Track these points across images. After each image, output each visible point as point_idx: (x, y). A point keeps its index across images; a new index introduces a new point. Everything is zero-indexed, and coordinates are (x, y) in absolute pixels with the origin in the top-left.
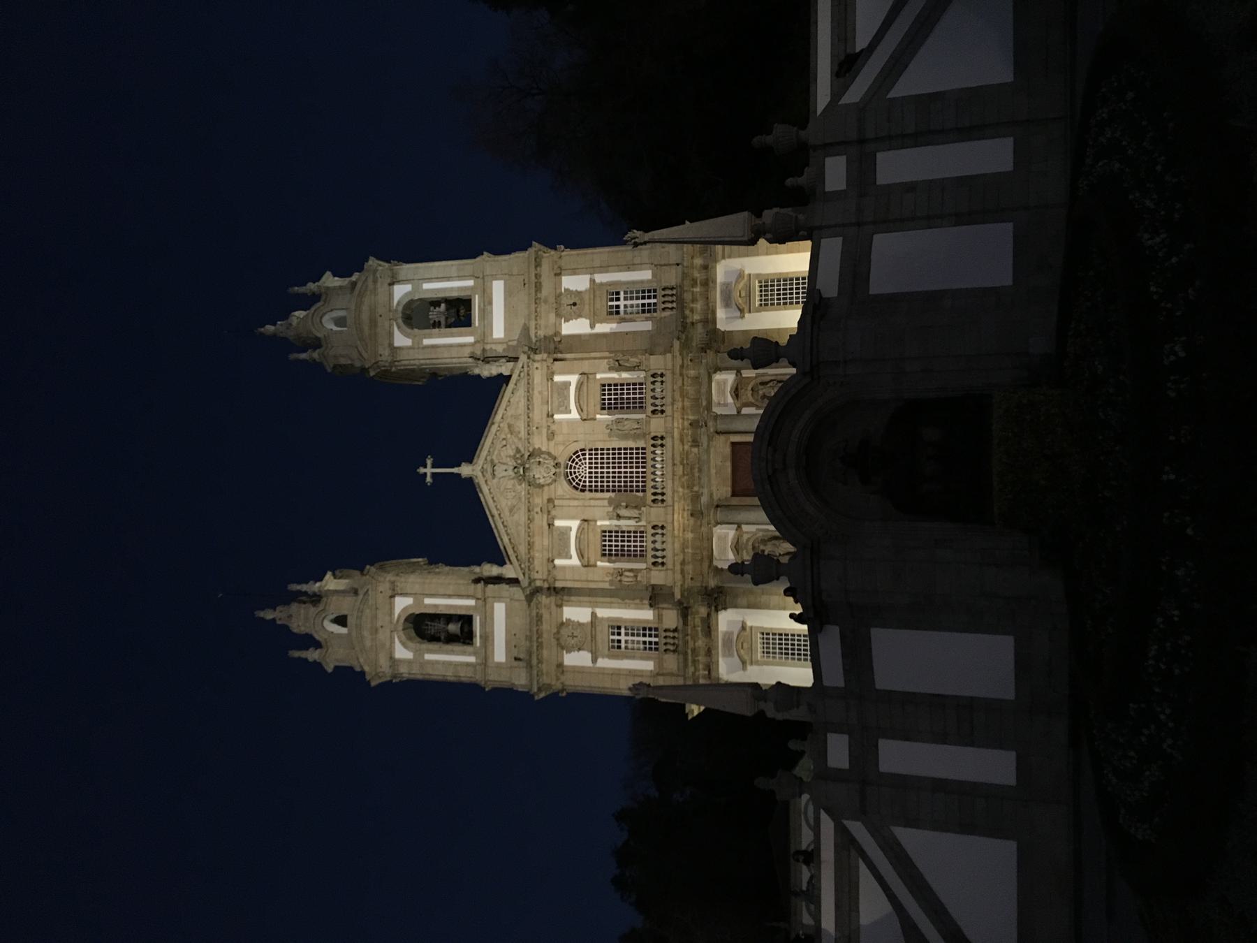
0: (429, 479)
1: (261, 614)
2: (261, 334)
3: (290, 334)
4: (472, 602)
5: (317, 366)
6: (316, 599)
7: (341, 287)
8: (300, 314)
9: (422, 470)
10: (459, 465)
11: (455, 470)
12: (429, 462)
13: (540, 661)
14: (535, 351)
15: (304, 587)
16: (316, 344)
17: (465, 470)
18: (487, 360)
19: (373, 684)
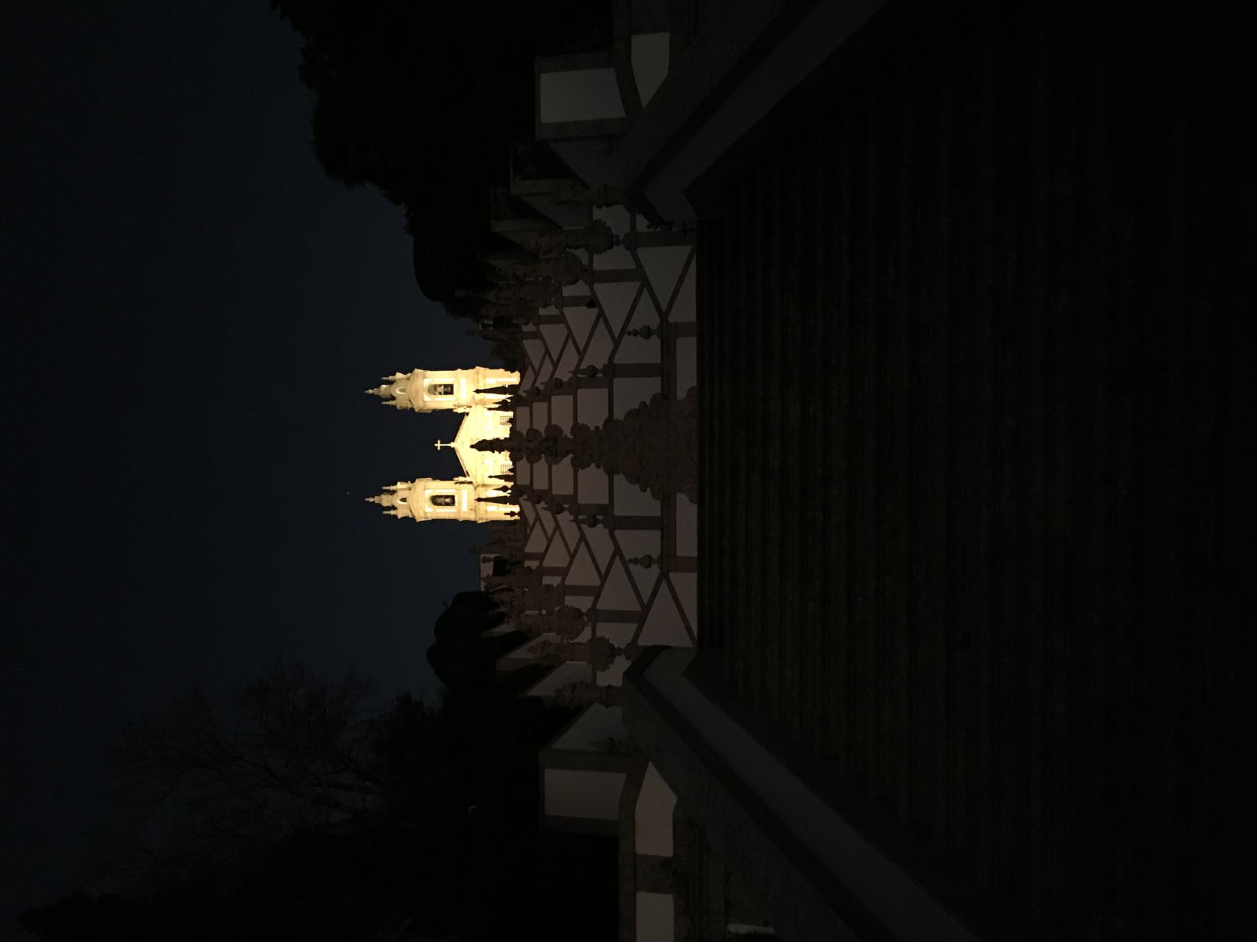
0: (439, 448)
1: (367, 500)
2: (368, 394)
3: (381, 394)
4: (455, 491)
5: (394, 407)
6: (394, 492)
7: (402, 379)
8: (384, 386)
9: (436, 445)
10: (450, 443)
11: (449, 445)
12: (439, 442)
13: (479, 510)
14: (477, 404)
15: (388, 488)
16: (393, 398)
17: (452, 445)
18: (459, 407)
19: (418, 521)
